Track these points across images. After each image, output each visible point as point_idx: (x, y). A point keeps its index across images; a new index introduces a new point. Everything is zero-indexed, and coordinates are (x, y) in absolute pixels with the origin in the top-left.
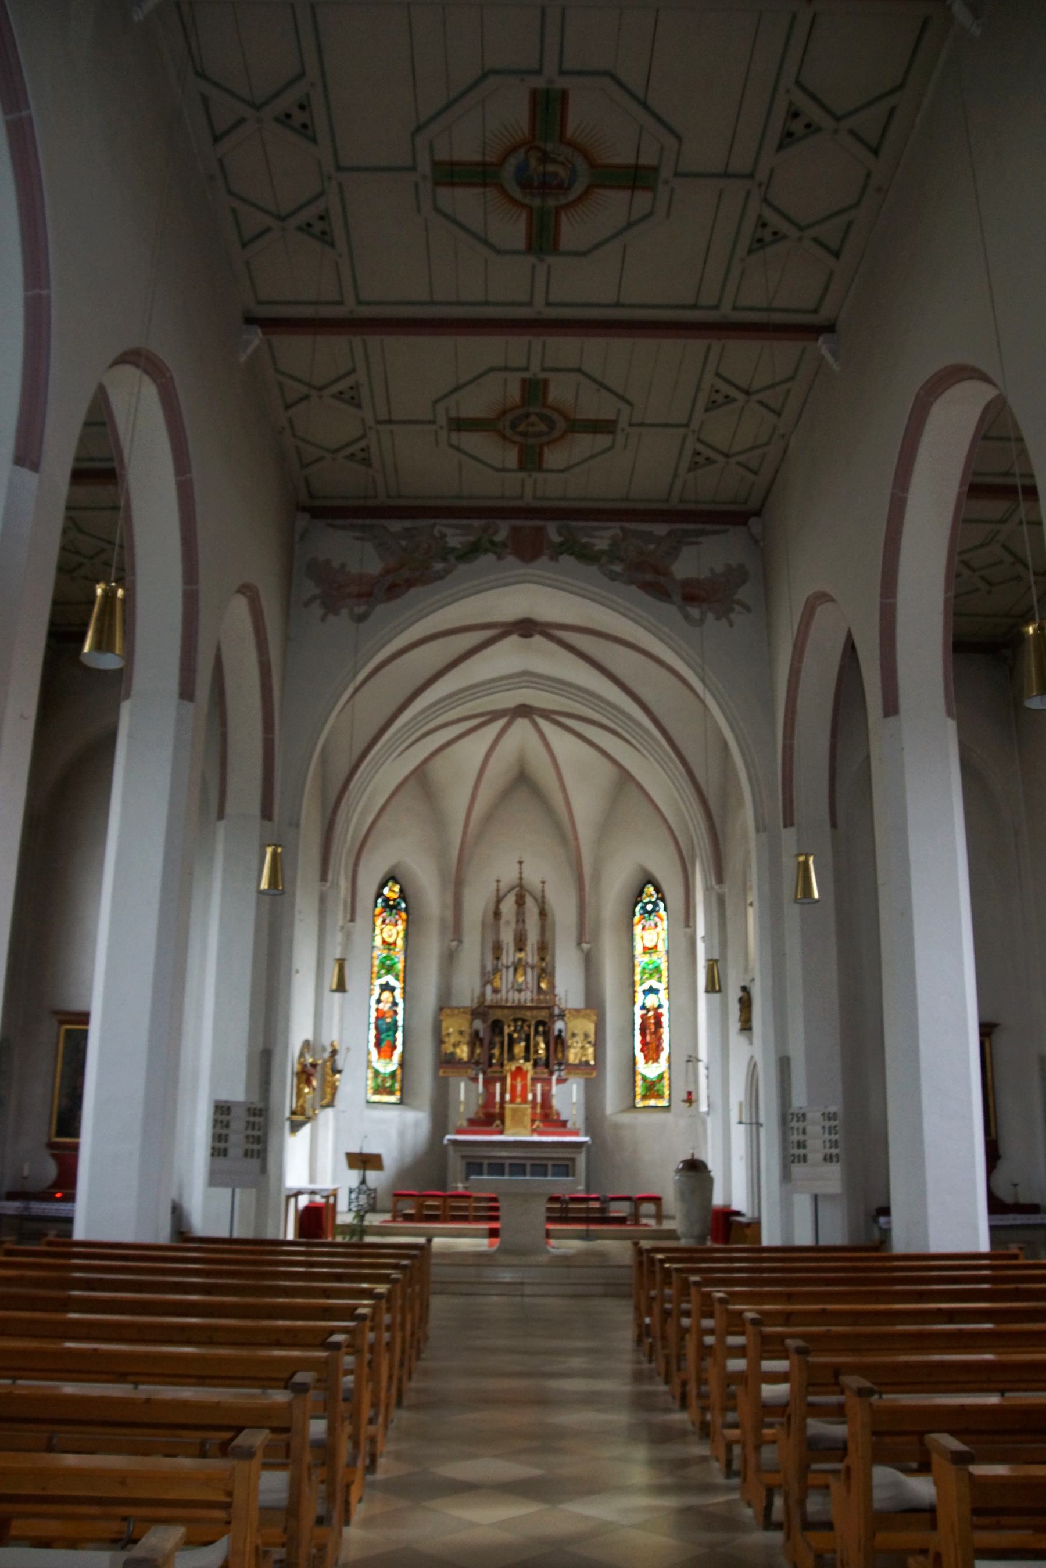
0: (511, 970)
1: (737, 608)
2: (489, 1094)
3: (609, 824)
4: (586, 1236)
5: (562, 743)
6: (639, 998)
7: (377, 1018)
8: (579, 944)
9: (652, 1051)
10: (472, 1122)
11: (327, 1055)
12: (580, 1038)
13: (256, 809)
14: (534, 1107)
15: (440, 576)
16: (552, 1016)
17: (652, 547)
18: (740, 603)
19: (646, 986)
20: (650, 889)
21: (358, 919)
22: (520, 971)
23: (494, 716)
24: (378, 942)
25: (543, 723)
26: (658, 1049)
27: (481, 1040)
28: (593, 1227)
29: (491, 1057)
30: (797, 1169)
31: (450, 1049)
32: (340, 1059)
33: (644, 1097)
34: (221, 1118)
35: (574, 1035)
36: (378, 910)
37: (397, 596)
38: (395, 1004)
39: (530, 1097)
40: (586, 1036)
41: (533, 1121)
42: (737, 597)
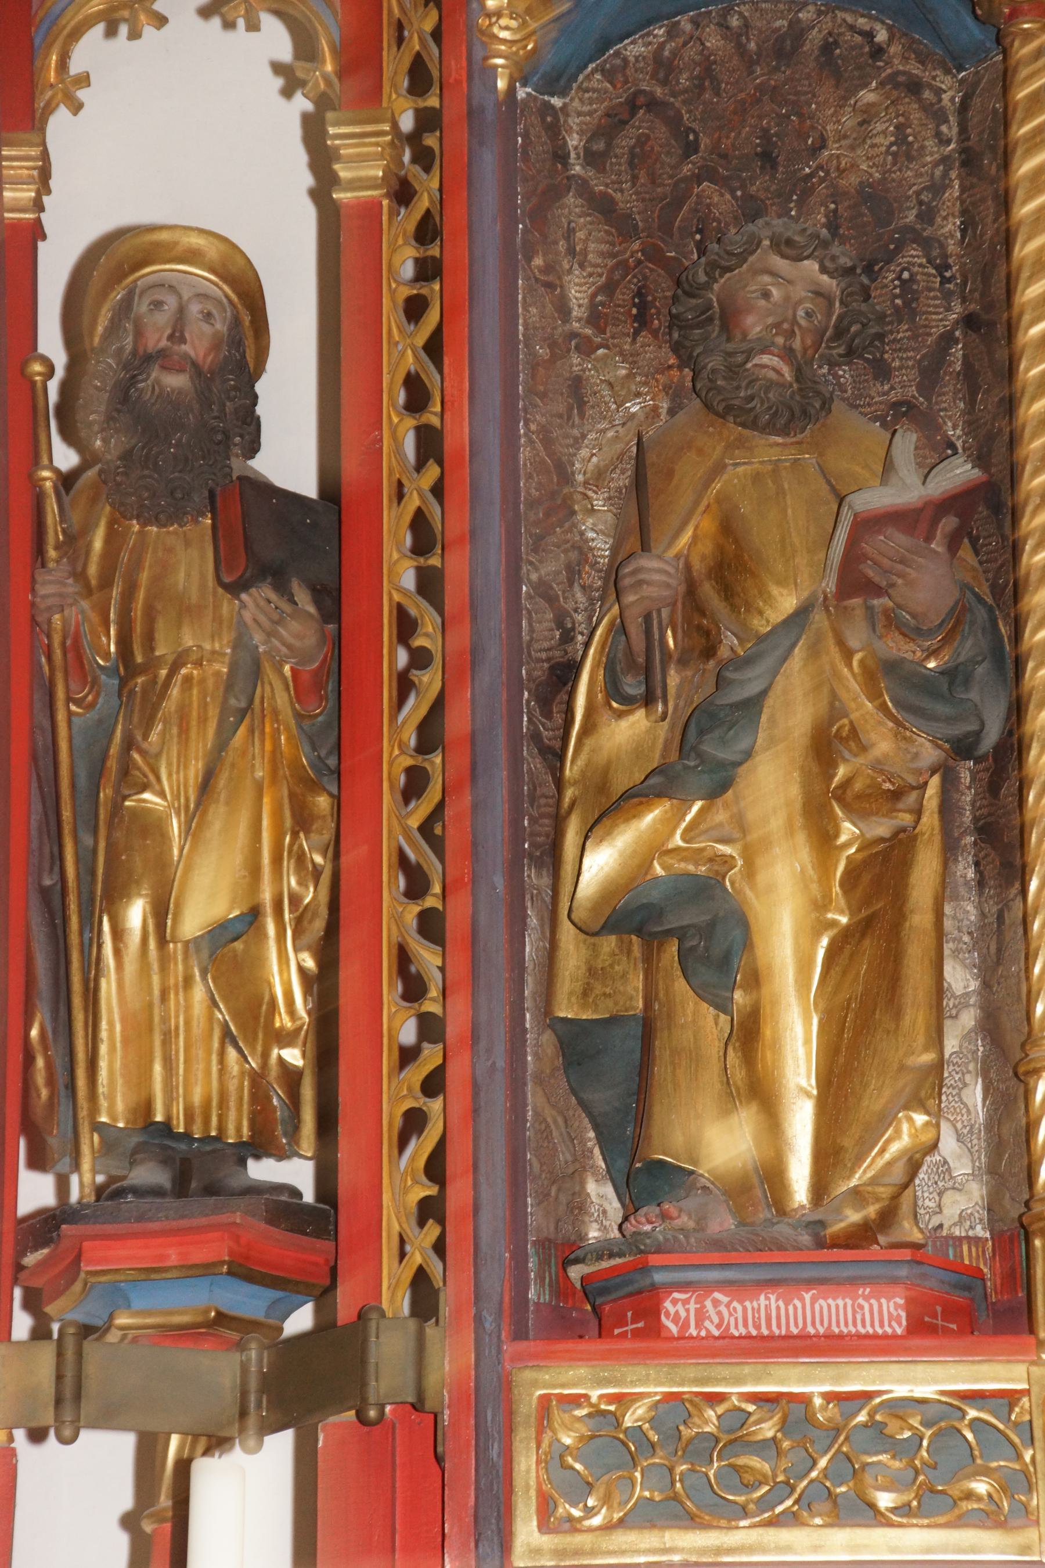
27: (290, 546)
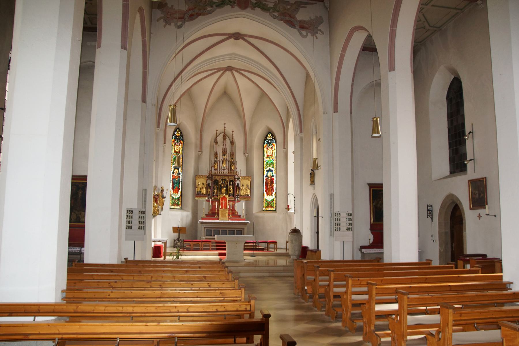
0: (221, 162)
1: (319, 32)
2: (213, 206)
3: (255, 112)
4: (253, 255)
5: (242, 81)
6: (265, 173)
7: (173, 179)
8: (244, 154)
9: (269, 191)
10: (206, 215)
11: (160, 191)
12: (245, 186)
13: (140, 99)
14: (229, 210)
15: (210, 13)
16: (235, 178)
17: (289, 7)
18: (320, 30)
19: (268, 169)
20: (270, 135)
22: (224, 162)
23: (219, 70)
24: (173, 151)
25: (235, 73)
26: (272, 191)
27: (210, 187)
28: (254, 252)
29: (214, 193)
30: (337, 233)
31: (199, 190)
32: (165, 193)
33: (266, 207)
34: (129, 215)
35: (243, 185)
36: (173, 140)
37: (193, 19)
38: (179, 174)
39: (228, 207)
40: (247, 186)
41: (229, 215)
42: (319, 28)
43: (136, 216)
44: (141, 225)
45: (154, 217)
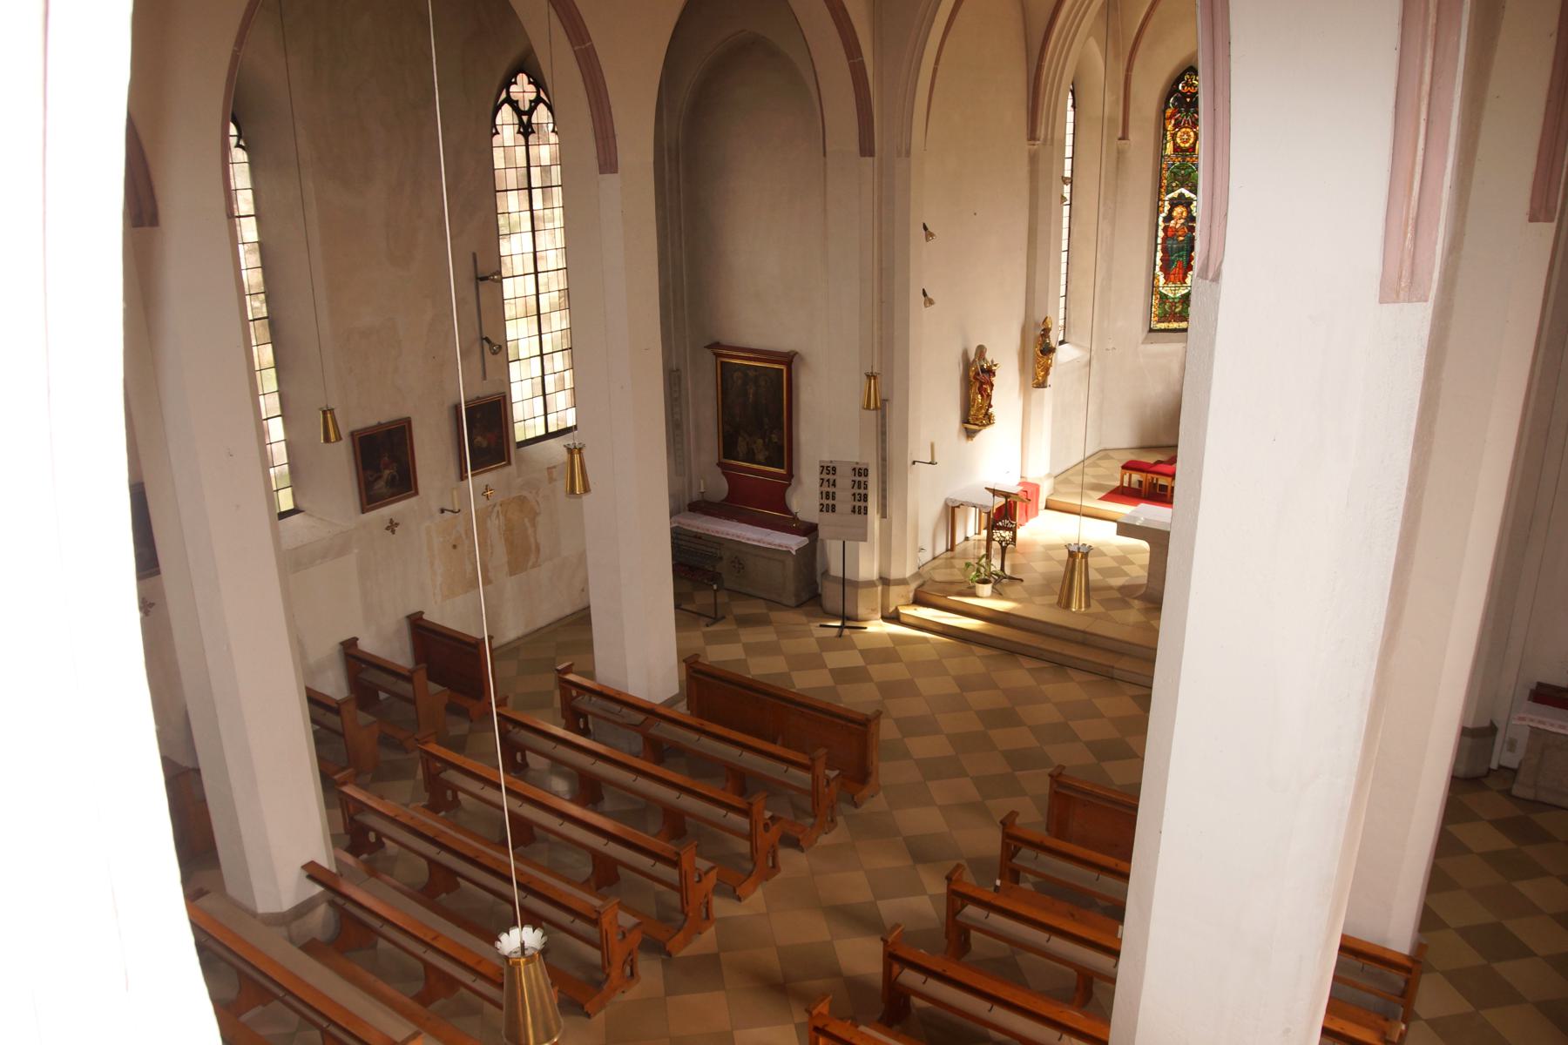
11: (1039, 332)
21: (1132, 135)
36: (1169, 112)
43: (844, 481)
44: (857, 504)
45: (970, 434)
